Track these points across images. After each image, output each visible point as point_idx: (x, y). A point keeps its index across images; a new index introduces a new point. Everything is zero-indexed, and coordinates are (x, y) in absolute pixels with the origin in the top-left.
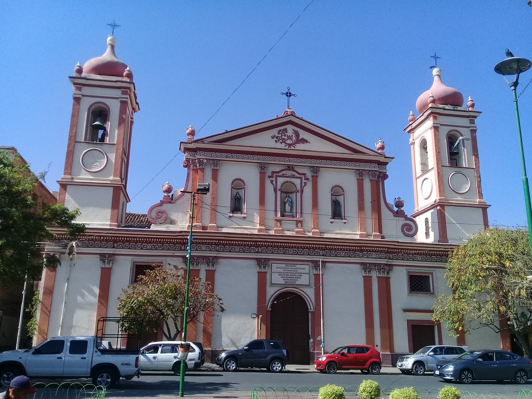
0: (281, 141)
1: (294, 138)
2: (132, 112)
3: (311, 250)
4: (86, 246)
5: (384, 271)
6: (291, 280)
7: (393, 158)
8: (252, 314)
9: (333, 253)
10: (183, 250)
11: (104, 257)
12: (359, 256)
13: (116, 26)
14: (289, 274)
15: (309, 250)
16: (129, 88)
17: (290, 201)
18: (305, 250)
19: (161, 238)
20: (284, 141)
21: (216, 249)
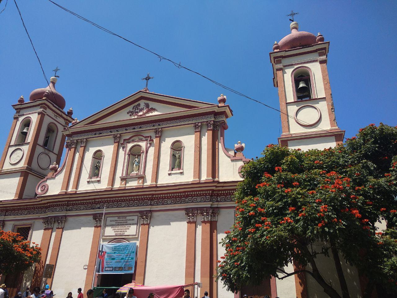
0: (135, 114)
6: (120, 231)
8: (85, 265)
9: (161, 202)
12: (184, 202)
15: (139, 202)
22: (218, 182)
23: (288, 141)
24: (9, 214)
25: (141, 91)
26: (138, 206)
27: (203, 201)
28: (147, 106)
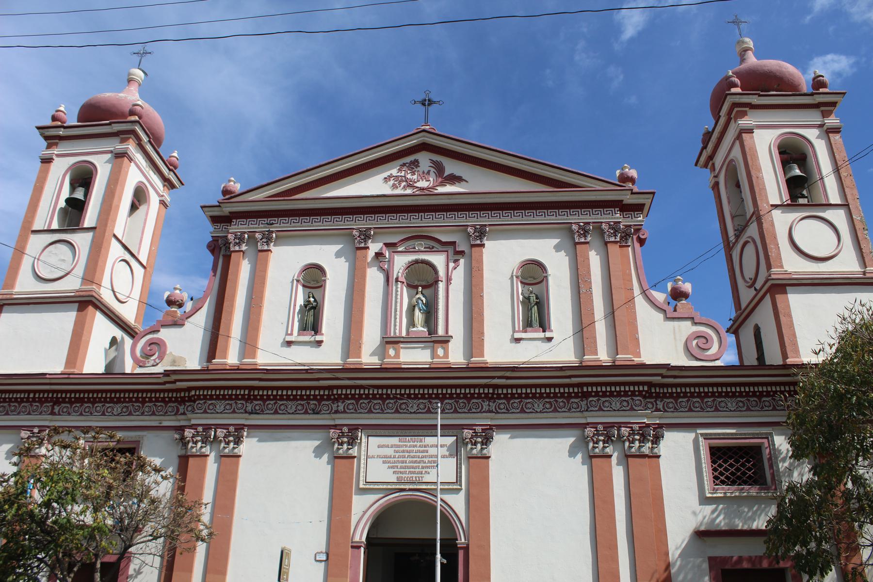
0: (404, 184)
2: (164, 186)
3: (461, 401)
5: (642, 439)
7: (653, 193)
9: (515, 405)
10: (182, 414)
13: (146, 53)
14: (408, 460)
15: (457, 402)
16: (133, 132)
17: (424, 302)
19: (138, 391)
20: (411, 183)
21: (245, 410)
22: (643, 366)
23: (787, 288)
24: (65, 410)
25: (424, 131)
26: (456, 411)
27: (628, 408)
28: (439, 169)
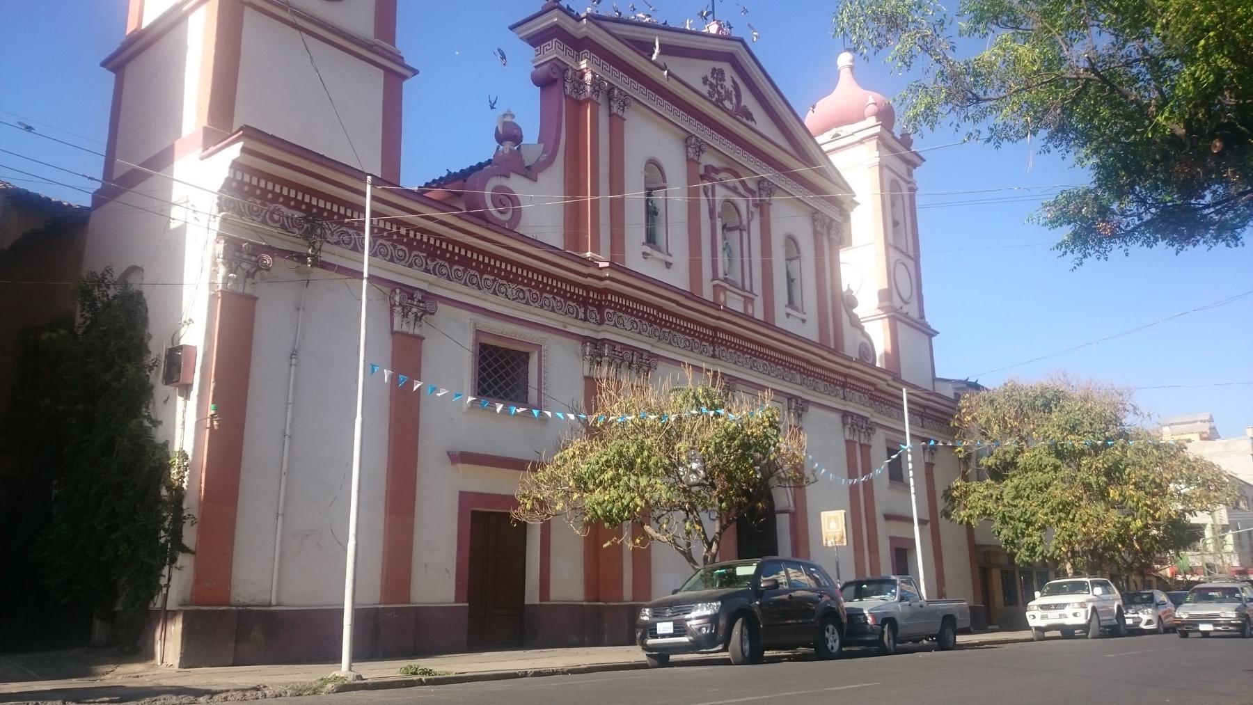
1: (734, 100)
4: (351, 245)
10: (581, 319)
11: (409, 298)
18: (779, 367)
